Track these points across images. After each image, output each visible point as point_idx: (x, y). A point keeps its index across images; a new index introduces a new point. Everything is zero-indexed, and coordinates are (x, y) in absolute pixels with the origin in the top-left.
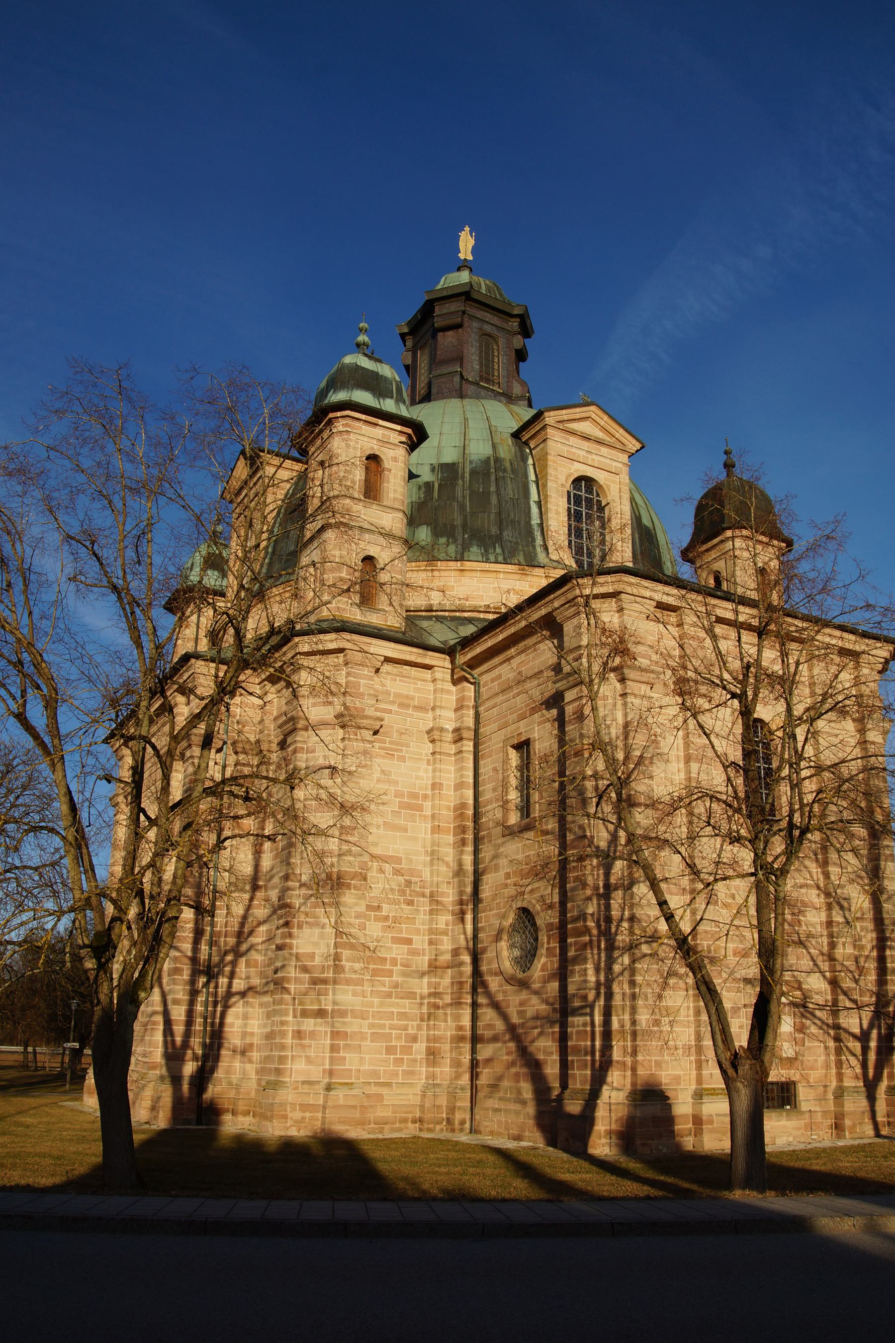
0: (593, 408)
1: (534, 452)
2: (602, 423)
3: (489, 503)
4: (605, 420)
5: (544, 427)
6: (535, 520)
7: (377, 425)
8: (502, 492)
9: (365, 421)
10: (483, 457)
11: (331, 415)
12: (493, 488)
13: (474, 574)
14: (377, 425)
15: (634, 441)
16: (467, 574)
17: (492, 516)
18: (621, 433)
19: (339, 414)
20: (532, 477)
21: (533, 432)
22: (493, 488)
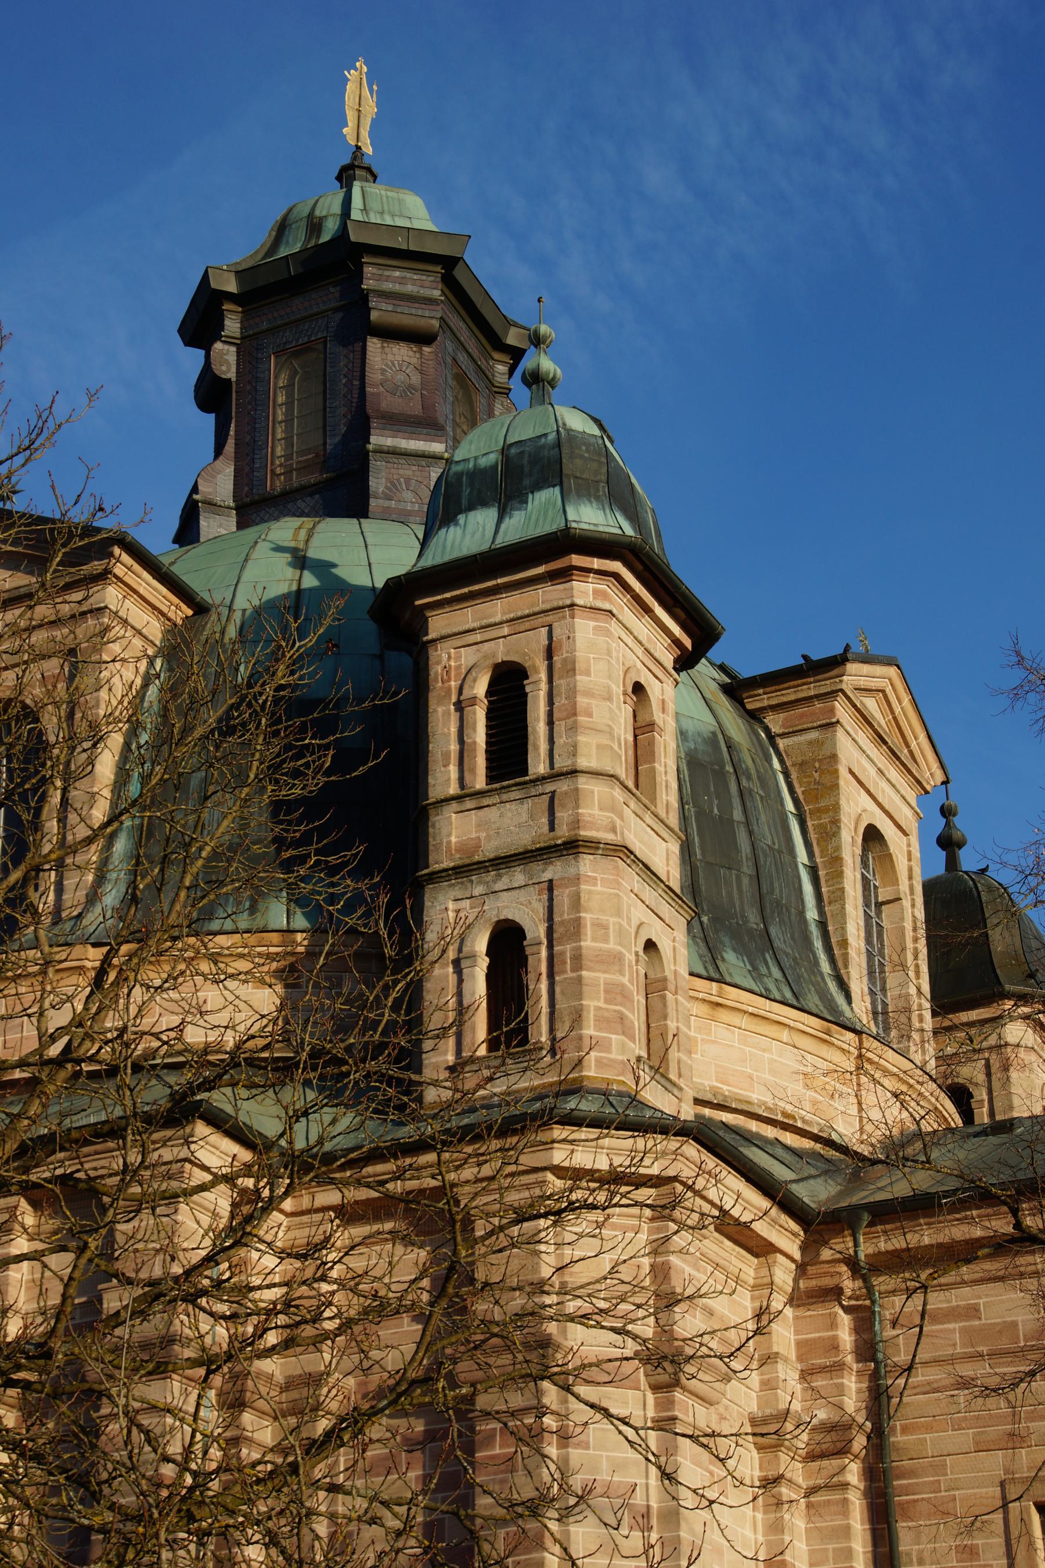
0: (892, 671)
1: (781, 743)
2: (898, 710)
3: (738, 850)
4: (903, 705)
5: (833, 694)
6: (812, 914)
7: (648, 610)
8: (755, 828)
9: (637, 598)
10: (706, 734)
11: (577, 560)
12: (737, 815)
13: (736, 1019)
14: (648, 610)
15: (935, 766)
16: (724, 1015)
17: (745, 881)
18: (920, 742)
19: (596, 563)
20: (790, 806)
21: (790, 695)
22: (737, 815)
